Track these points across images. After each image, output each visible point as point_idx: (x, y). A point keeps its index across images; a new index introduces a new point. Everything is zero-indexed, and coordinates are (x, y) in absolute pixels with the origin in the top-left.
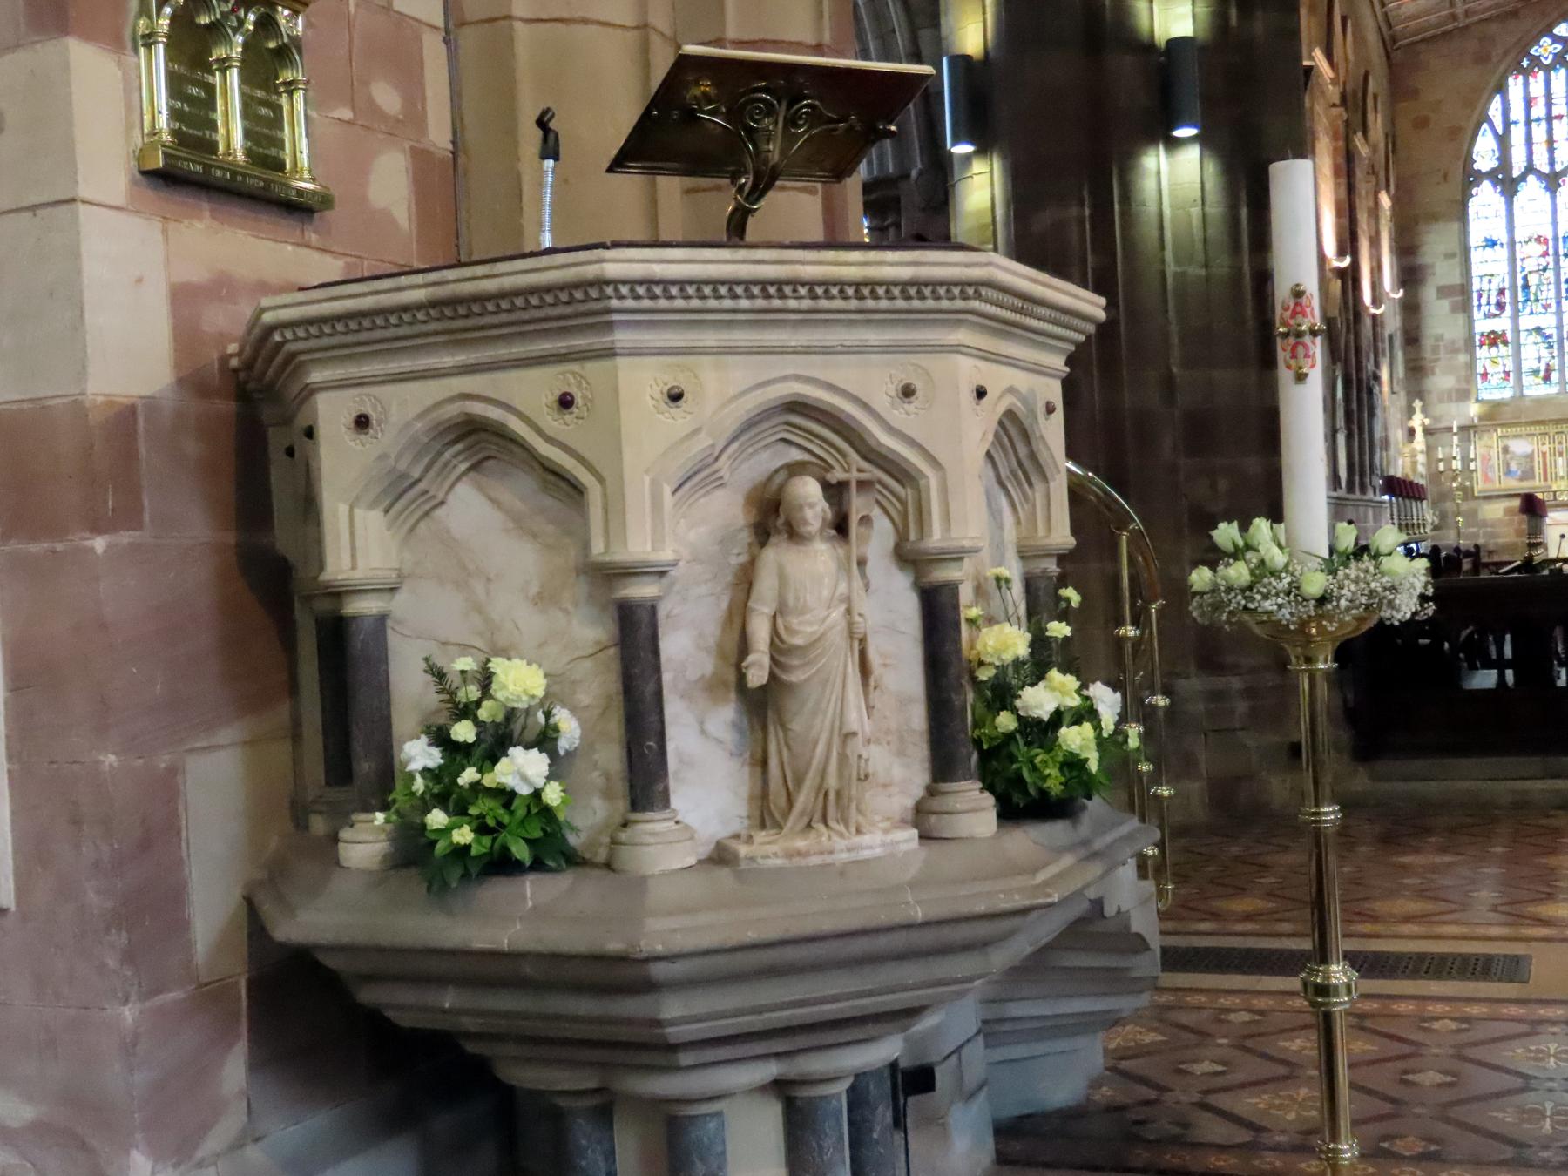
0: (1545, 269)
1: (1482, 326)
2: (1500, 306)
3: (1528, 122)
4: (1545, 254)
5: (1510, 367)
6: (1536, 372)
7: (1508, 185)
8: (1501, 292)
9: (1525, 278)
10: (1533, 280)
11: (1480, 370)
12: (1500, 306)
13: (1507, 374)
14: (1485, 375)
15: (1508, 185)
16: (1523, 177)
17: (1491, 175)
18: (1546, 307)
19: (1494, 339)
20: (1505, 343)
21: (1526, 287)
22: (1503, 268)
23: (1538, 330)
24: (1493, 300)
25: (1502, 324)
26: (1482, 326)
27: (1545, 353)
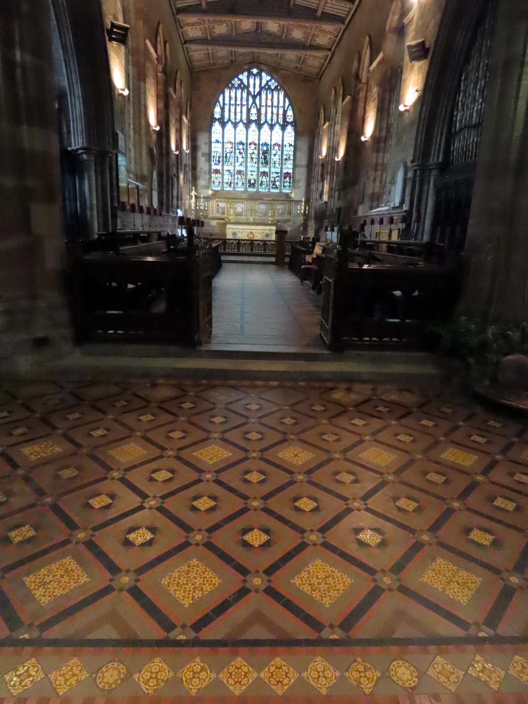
0: (232, 152)
1: (214, 167)
2: (219, 161)
3: (230, 104)
4: (232, 148)
5: (221, 181)
6: (227, 183)
7: (223, 125)
8: (219, 157)
9: (226, 154)
10: (228, 155)
11: (212, 180)
12: (219, 161)
13: (220, 182)
14: (214, 182)
15: (223, 125)
16: (227, 122)
17: (219, 120)
18: (231, 164)
19: (217, 171)
20: (220, 173)
21: (226, 157)
22: (220, 150)
23: (229, 171)
24: (217, 160)
25: (219, 167)
26: (214, 167)
27: (230, 178)
